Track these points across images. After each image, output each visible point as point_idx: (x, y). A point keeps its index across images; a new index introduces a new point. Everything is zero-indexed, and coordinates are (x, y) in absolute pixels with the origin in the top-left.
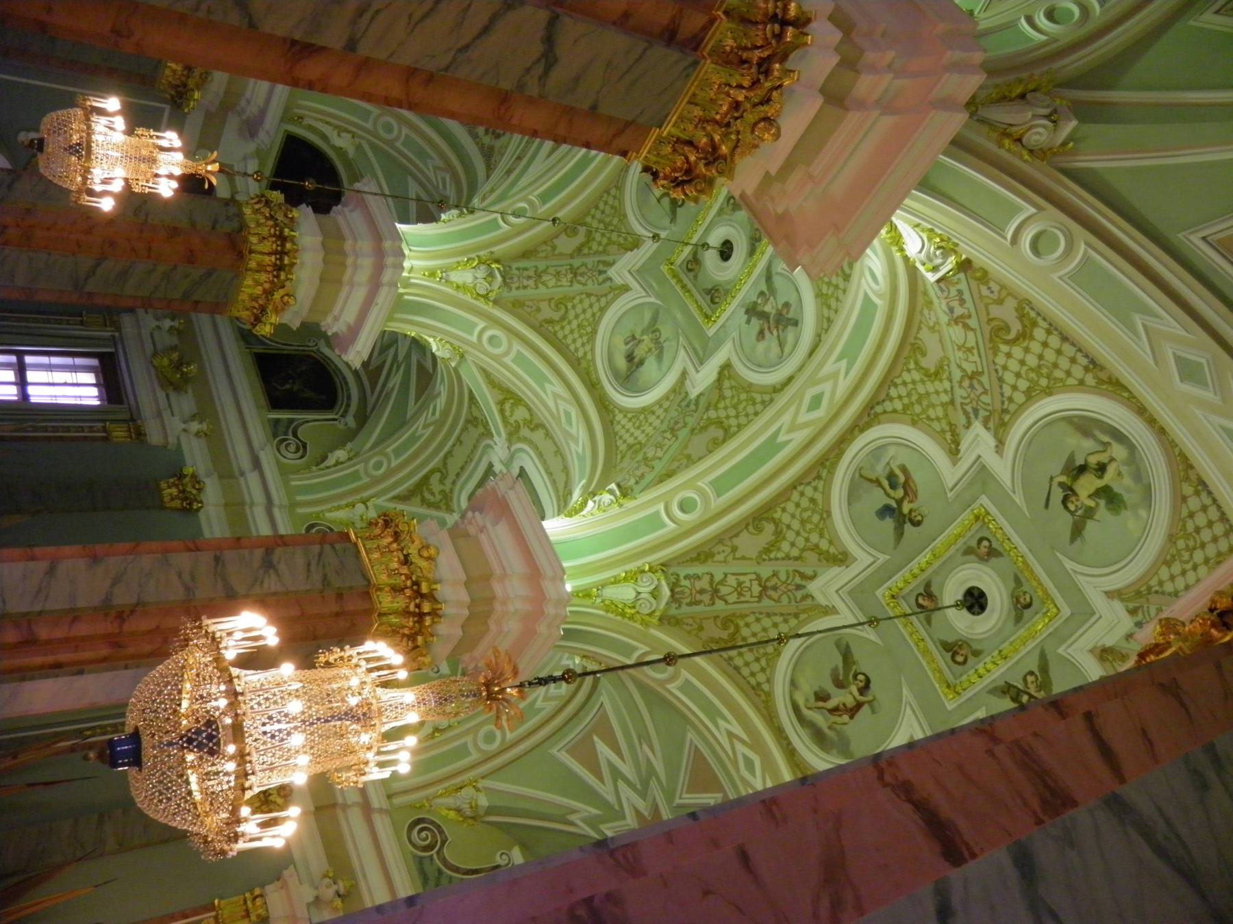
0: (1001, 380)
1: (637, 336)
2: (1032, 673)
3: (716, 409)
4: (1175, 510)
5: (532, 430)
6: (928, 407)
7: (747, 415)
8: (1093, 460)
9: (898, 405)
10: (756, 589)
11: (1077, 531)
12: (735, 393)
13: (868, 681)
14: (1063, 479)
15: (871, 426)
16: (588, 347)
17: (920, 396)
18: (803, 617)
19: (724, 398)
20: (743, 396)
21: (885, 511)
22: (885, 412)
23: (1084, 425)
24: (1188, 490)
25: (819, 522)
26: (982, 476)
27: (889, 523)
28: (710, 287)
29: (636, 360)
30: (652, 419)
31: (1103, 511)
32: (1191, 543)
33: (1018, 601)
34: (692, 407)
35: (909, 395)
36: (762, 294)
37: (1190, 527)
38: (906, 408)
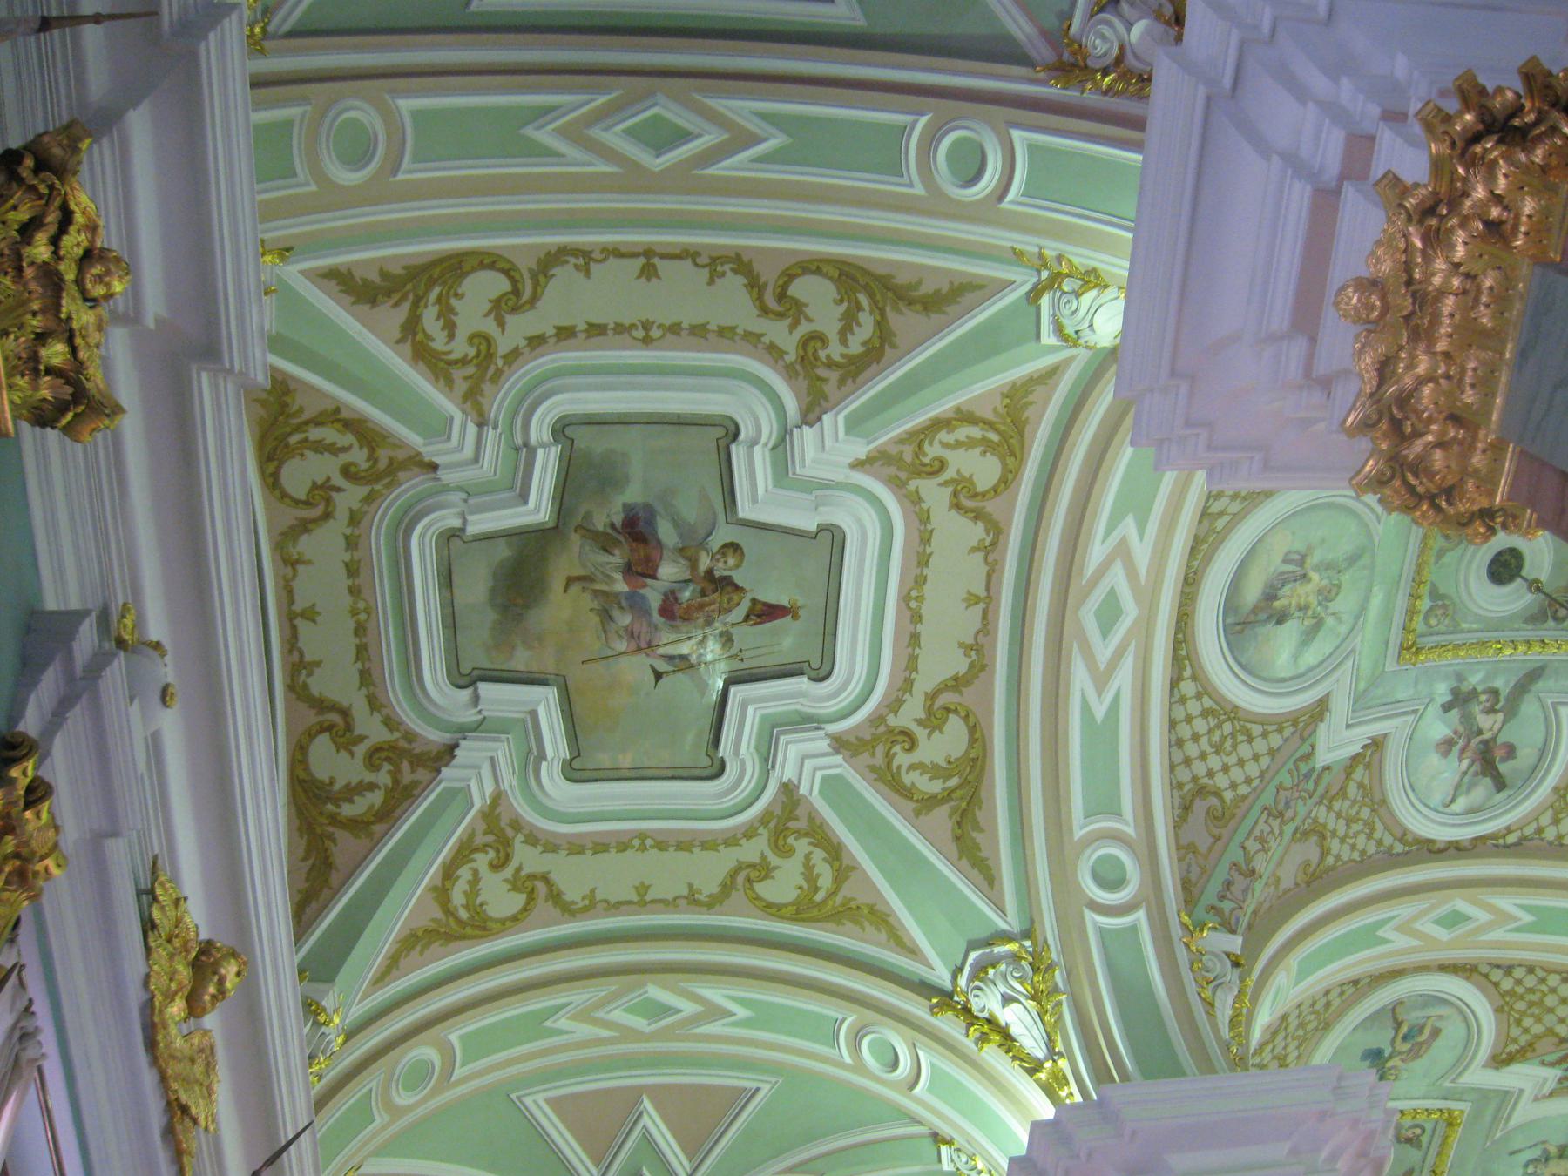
1: (1309, 562)
3: (1329, 808)
5: (957, 506)
6: (1532, 1015)
7: (1353, 847)
12: (1360, 799)
16: (1235, 507)
17: (1540, 1003)
19: (1345, 797)
20: (1365, 813)
22: (1486, 976)
28: (1442, 591)
29: (1277, 604)
30: (1245, 751)
34: (1310, 786)
35: (1530, 990)
36: (1495, 693)
38: (1511, 993)
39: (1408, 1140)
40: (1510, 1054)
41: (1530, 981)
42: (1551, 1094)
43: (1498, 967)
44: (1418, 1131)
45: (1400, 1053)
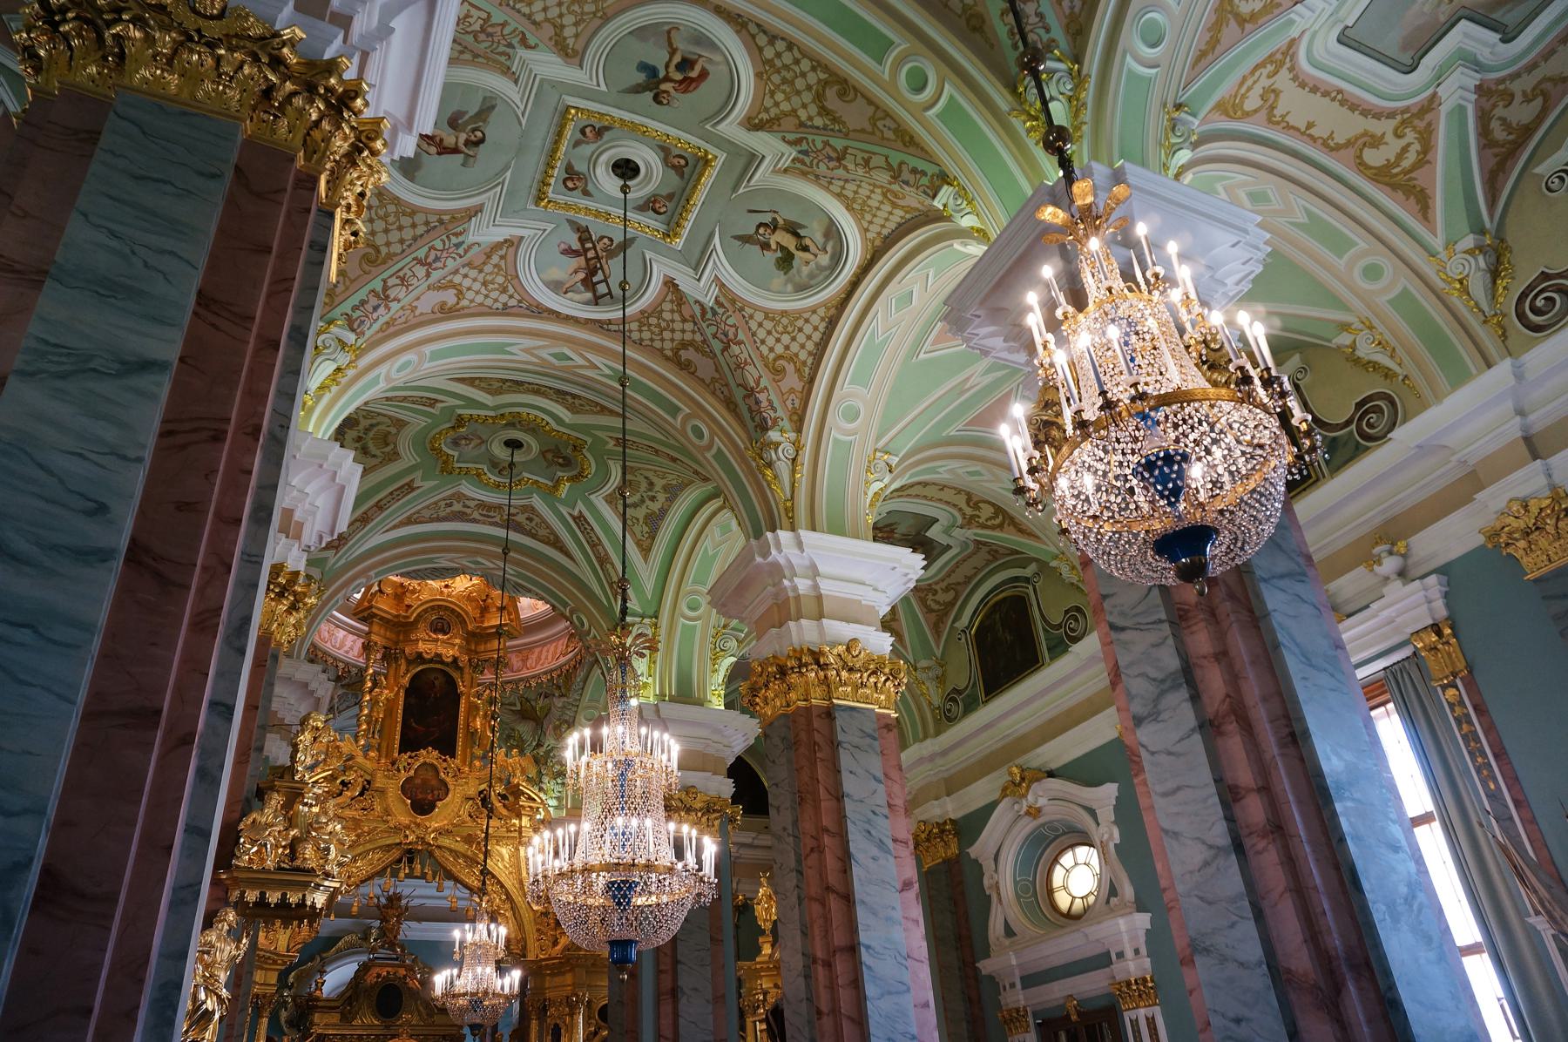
0: (846, 181)
2: (611, 240)
4: (804, 310)
6: (784, 92)
8: (807, 242)
9: (769, 53)
10: (477, 27)
11: (745, 239)
13: (482, 141)
14: (781, 222)
15: (729, 23)
17: (792, 83)
18: (480, 60)
21: (650, 70)
23: (832, 232)
24: (821, 312)
25: (588, 14)
26: (752, 160)
27: (641, 77)
31: (771, 257)
32: (790, 329)
33: (654, 202)
35: (786, 67)
37: (800, 323)
38: (770, 62)
39: (674, 167)
40: (762, 120)
41: (787, 58)
42: (786, 171)
43: (765, 32)
44: (682, 162)
45: (672, 80)
